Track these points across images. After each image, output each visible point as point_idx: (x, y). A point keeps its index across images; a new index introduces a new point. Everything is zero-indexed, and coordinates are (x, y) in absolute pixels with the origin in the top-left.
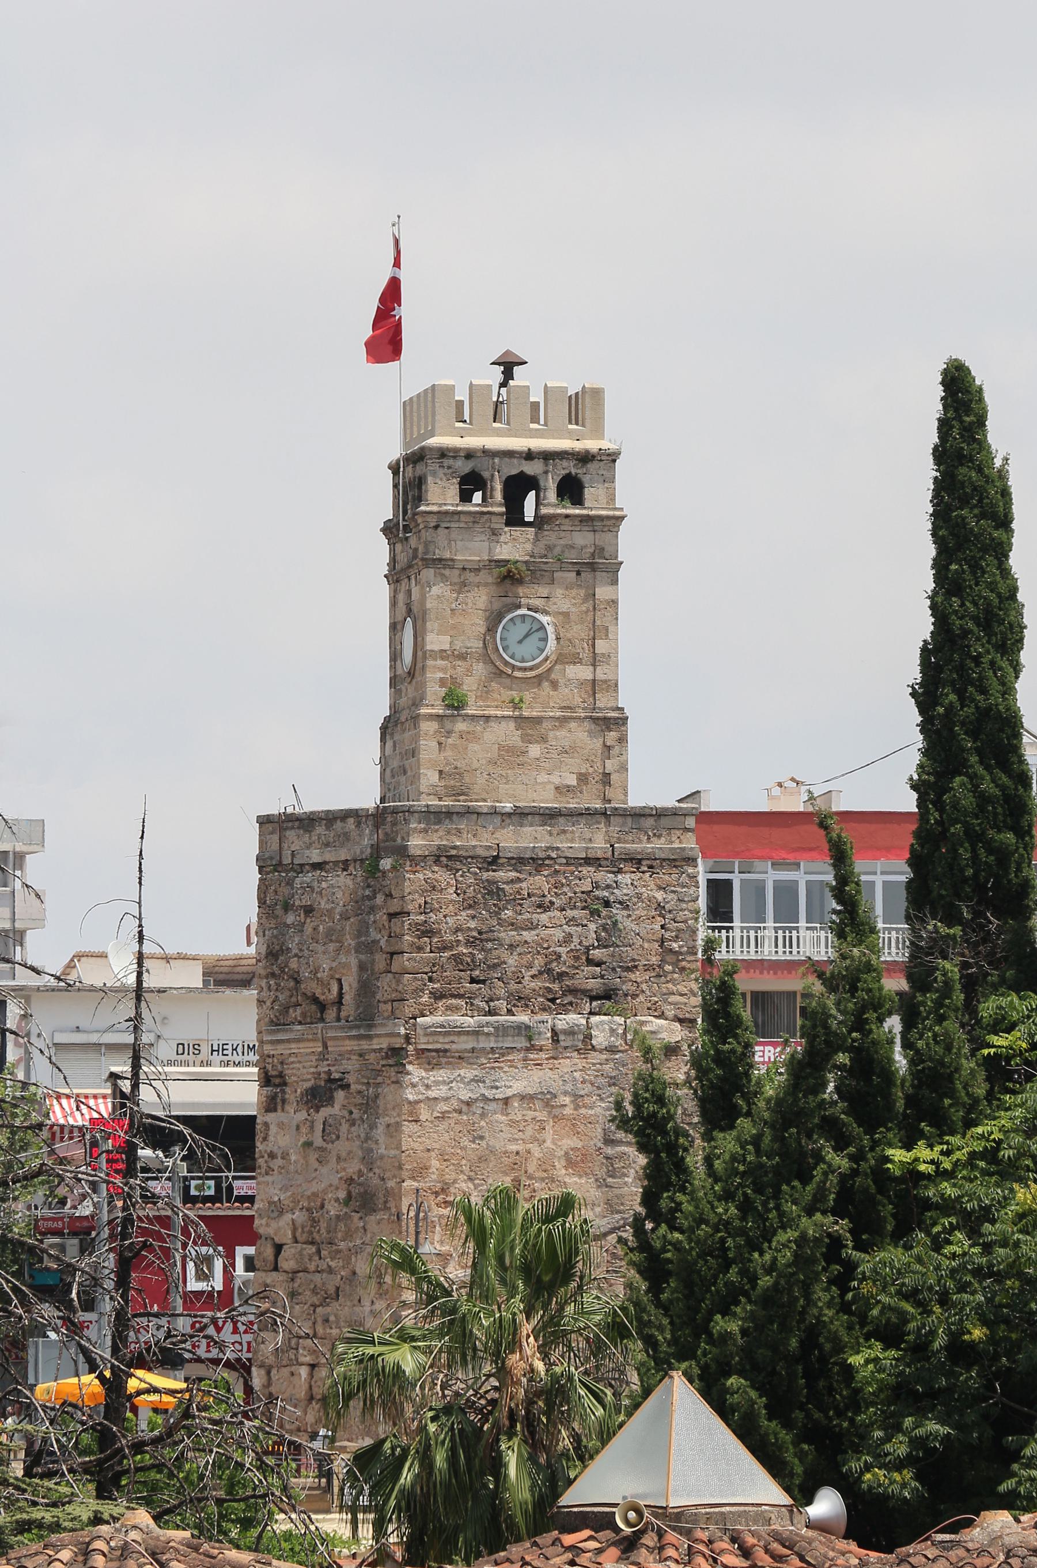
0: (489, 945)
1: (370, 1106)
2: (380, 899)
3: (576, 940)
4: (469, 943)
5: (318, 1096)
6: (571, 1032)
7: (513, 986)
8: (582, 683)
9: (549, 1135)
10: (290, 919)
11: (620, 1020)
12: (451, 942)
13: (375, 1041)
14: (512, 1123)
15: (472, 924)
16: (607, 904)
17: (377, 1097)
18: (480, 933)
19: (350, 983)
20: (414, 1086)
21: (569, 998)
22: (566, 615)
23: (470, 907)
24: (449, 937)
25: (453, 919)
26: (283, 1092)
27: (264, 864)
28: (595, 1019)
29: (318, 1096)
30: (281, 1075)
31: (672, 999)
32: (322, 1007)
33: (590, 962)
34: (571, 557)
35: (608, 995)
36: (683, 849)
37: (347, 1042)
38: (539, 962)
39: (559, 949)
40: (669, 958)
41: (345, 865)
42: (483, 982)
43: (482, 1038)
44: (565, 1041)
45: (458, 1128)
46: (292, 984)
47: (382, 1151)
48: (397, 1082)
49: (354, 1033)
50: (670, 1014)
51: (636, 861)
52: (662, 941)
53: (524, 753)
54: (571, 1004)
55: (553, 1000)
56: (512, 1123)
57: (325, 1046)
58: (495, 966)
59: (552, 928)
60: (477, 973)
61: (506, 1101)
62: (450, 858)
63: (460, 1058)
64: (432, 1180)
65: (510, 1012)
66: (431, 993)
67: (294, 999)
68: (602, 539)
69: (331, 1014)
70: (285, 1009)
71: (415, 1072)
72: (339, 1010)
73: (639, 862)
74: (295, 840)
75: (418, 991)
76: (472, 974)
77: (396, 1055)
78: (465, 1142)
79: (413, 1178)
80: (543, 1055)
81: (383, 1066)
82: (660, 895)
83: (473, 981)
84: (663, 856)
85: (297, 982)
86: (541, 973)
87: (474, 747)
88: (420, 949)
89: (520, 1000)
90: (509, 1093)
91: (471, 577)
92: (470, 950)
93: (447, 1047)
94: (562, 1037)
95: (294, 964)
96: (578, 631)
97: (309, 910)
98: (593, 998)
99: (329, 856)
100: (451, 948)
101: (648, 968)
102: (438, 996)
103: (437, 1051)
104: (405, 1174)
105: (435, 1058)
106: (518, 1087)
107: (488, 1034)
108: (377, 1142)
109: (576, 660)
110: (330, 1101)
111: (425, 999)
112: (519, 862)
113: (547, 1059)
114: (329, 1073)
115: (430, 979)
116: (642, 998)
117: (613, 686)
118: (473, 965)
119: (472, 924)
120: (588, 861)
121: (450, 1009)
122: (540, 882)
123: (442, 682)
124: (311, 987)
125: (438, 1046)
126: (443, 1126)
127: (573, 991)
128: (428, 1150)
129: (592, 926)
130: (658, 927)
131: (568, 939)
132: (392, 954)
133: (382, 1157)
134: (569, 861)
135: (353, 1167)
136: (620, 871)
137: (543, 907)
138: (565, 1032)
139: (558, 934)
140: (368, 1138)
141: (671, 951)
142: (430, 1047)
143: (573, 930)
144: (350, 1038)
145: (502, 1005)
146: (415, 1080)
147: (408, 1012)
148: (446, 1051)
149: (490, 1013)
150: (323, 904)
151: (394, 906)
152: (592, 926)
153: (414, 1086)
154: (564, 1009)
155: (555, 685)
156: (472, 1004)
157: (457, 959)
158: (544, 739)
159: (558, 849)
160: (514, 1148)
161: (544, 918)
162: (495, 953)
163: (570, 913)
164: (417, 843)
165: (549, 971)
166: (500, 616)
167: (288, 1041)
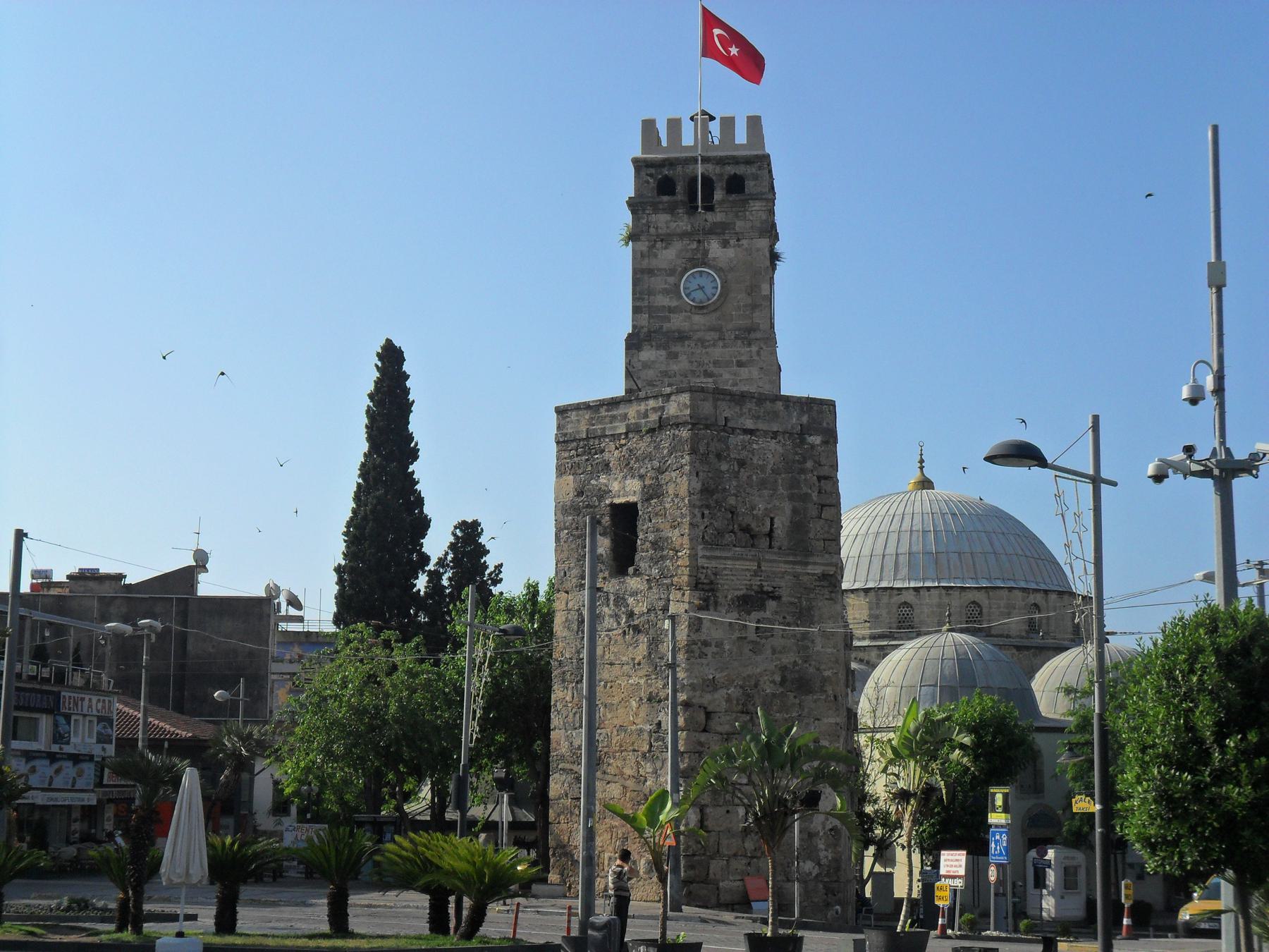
19: (781, 524)
29: (750, 602)
41: (775, 435)
47: (818, 648)
99: (762, 426)
108: (813, 641)
110: (762, 607)
114: (761, 586)
132: (823, 506)
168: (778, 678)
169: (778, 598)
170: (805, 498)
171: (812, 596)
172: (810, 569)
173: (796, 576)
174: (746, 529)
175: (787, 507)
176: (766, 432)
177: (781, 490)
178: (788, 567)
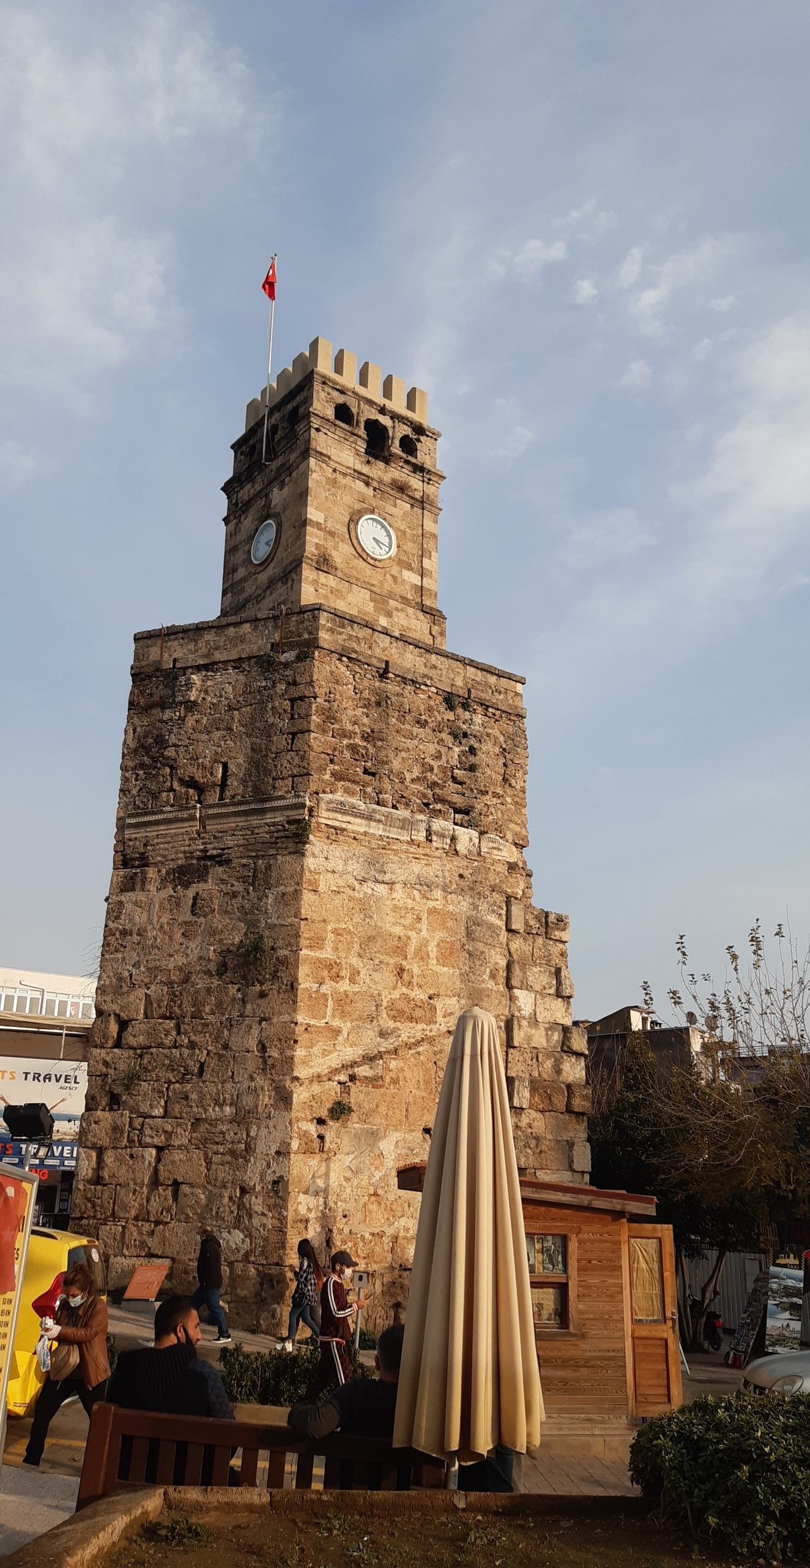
0: (380, 743)
1: (258, 880)
2: (281, 687)
3: (444, 758)
4: (366, 738)
9: (424, 926)
12: (350, 732)
13: (268, 816)
14: (396, 909)
15: (366, 720)
16: (465, 735)
17: (269, 867)
18: (372, 732)
21: (439, 806)
23: (365, 706)
24: (349, 727)
27: (138, 676)
31: (511, 826)
32: (201, 789)
33: (454, 779)
36: (517, 707)
37: (232, 819)
39: (432, 763)
40: (509, 791)
42: (373, 774)
43: (373, 824)
44: (437, 842)
45: (351, 905)
49: (242, 808)
50: (509, 836)
54: (440, 811)
60: (369, 764)
61: (392, 884)
63: (355, 838)
65: (394, 807)
66: (332, 774)
69: (213, 797)
71: (316, 845)
75: (322, 769)
78: (358, 918)
80: (420, 850)
81: (277, 838)
83: (366, 772)
84: (503, 708)
86: (418, 778)
89: (402, 800)
92: (365, 744)
93: (344, 826)
94: (434, 838)
100: (350, 738)
103: (335, 828)
104: (303, 942)
107: (379, 821)
111: (327, 777)
113: (425, 855)
115: (332, 761)
116: (491, 817)
118: (365, 757)
125: (337, 824)
128: (324, 921)
129: (457, 749)
131: (438, 757)
132: (294, 735)
137: (423, 724)
139: (432, 748)
142: (329, 822)
143: (443, 750)
147: (313, 787)
148: (345, 830)
149: (378, 803)
150: (209, 699)
156: (365, 792)
157: (353, 748)
159: (431, 679)
160: (397, 930)
162: (384, 753)
167: (157, 823)
170: (268, 731)
171: (272, 852)
172: (269, 818)
176: (225, 662)
178: (241, 822)
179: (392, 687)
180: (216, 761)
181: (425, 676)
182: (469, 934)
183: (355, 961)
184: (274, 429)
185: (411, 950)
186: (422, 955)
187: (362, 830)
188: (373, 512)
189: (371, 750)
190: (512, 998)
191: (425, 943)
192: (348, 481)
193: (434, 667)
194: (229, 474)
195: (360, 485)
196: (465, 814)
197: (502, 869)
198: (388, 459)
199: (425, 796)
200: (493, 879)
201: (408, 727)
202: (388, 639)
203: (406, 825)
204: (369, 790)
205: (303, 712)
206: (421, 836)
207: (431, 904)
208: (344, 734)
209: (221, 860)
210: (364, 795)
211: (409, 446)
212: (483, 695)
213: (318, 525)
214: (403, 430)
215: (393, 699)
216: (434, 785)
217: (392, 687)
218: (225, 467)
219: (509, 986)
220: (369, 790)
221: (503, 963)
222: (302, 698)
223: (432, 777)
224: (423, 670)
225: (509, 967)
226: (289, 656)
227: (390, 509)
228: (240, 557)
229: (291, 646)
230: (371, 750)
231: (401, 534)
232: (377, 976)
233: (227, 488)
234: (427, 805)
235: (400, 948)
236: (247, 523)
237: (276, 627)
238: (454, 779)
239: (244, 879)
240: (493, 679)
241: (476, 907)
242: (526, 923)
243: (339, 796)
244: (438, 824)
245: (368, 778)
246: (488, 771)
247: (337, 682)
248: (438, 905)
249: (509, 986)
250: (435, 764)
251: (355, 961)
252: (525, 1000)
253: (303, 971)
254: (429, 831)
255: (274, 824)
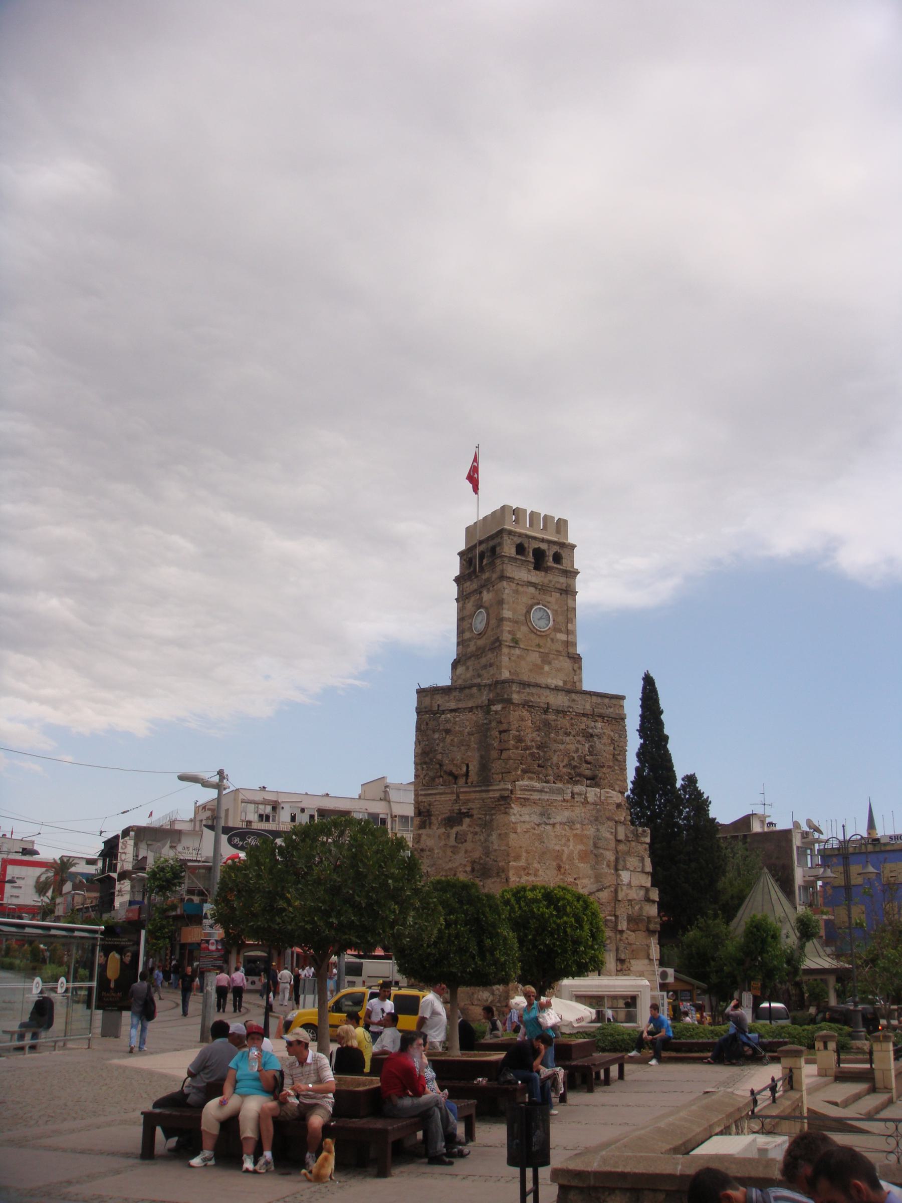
1: (487, 825)
2: (494, 724)
4: (538, 748)
5: (452, 820)
6: (580, 794)
7: (556, 771)
8: (563, 642)
9: (571, 844)
10: (436, 736)
11: (598, 790)
14: (556, 836)
15: (538, 739)
16: (592, 736)
17: (492, 820)
19: (474, 768)
20: (514, 815)
21: (578, 778)
22: (556, 611)
24: (529, 744)
25: (531, 736)
26: (430, 819)
28: (589, 789)
29: (452, 820)
30: (428, 811)
31: (618, 782)
32: (456, 777)
33: (587, 762)
34: (558, 586)
35: (592, 778)
38: (566, 761)
40: (617, 763)
41: (471, 709)
44: (577, 798)
46: (438, 766)
47: (496, 847)
48: (506, 813)
49: (477, 789)
50: (617, 788)
51: (602, 716)
52: (614, 755)
53: (543, 668)
55: (571, 778)
56: (556, 836)
57: (458, 797)
58: (548, 760)
59: (571, 744)
61: (554, 825)
62: (529, 706)
64: (522, 863)
65: (554, 783)
67: (439, 774)
68: (570, 581)
69: (462, 781)
70: (433, 779)
71: (516, 808)
72: (467, 779)
73: (603, 718)
74: (439, 700)
75: (516, 769)
76: (538, 763)
77: (505, 800)
78: (537, 844)
79: (514, 861)
80: (569, 804)
82: (612, 734)
83: (539, 766)
85: (441, 765)
87: (523, 663)
88: (517, 748)
90: (555, 821)
91: (521, 589)
95: (439, 757)
96: (561, 619)
97: (448, 731)
98: (587, 779)
99: (461, 705)
101: (609, 767)
102: (525, 771)
103: (524, 799)
105: (524, 802)
106: (559, 819)
108: (492, 843)
109: (560, 631)
110: (460, 823)
111: (519, 772)
112: (558, 712)
114: (460, 810)
117: (574, 645)
118: (539, 759)
119: (538, 739)
120: (584, 715)
121: (531, 779)
122: (564, 722)
123: (509, 632)
124: (448, 767)
126: (527, 835)
127: (580, 775)
130: (612, 748)
131: (577, 751)
132: (502, 751)
133: (496, 850)
134: (578, 714)
135: (476, 855)
136: (596, 721)
137: (568, 734)
138: (578, 794)
139: (572, 747)
140: (486, 840)
141: (617, 760)
143: (580, 746)
144: (475, 792)
145: (551, 778)
146: (516, 812)
148: (528, 799)
149: (546, 782)
151: (504, 726)
152: (587, 745)
153: (514, 815)
154: (576, 783)
155: (552, 640)
157: (532, 754)
158: (550, 663)
160: (557, 848)
161: (568, 739)
163: (578, 738)
164: (516, 697)
165: (570, 764)
166: (531, 607)
168: (468, 869)
169: (472, 816)
171: (493, 812)
172: (491, 794)
173: (483, 800)
174: (450, 773)
175: (477, 755)
176: (465, 709)
177: (473, 745)
178: (477, 795)
179: (551, 717)
180: (463, 763)
181: (569, 707)
182: (596, 846)
183: (536, 865)
184: (482, 556)
185: (565, 857)
186: (570, 858)
187: (538, 798)
188: (538, 604)
189: (542, 754)
190: (618, 876)
191: (572, 852)
192: (525, 589)
193: (574, 700)
194: (457, 573)
195: (532, 590)
196: (594, 780)
197: (613, 807)
198: (547, 570)
199: (570, 773)
200: (607, 814)
201: (560, 737)
202: (548, 691)
203: (560, 792)
204: (541, 776)
205: (506, 739)
206: (568, 797)
207: (575, 832)
208: (527, 748)
209: (468, 815)
210: (539, 780)
211: (557, 558)
212: (601, 711)
213: (509, 619)
214: (555, 549)
215: (552, 723)
216: (575, 767)
217: (551, 717)
218: (455, 569)
219: (616, 870)
220: (541, 776)
221: (613, 858)
222: (505, 731)
223: (574, 763)
224: (567, 703)
225: (617, 860)
226: (498, 707)
227: (549, 599)
228: (466, 625)
229: (499, 702)
230: (542, 754)
231: (555, 612)
232: (548, 872)
233: (457, 580)
234: (571, 778)
235: (558, 856)
236: (470, 605)
237: (490, 690)
238: (587, 762)
239: (480, 825)
240: (606, 701)
241: (598, 830)
242: (626, 835)
243: (526, 782)
244: (578, 789)
245: (540, 769)
246: (605, 754)
247: (522, 720)
248: (578, 832)
249: (616, 870)
250: (575, 755)
251: (536, 865)
252: (625, 876)
253: (511, 873)
254: (573, 794)
255: (494, 798)
